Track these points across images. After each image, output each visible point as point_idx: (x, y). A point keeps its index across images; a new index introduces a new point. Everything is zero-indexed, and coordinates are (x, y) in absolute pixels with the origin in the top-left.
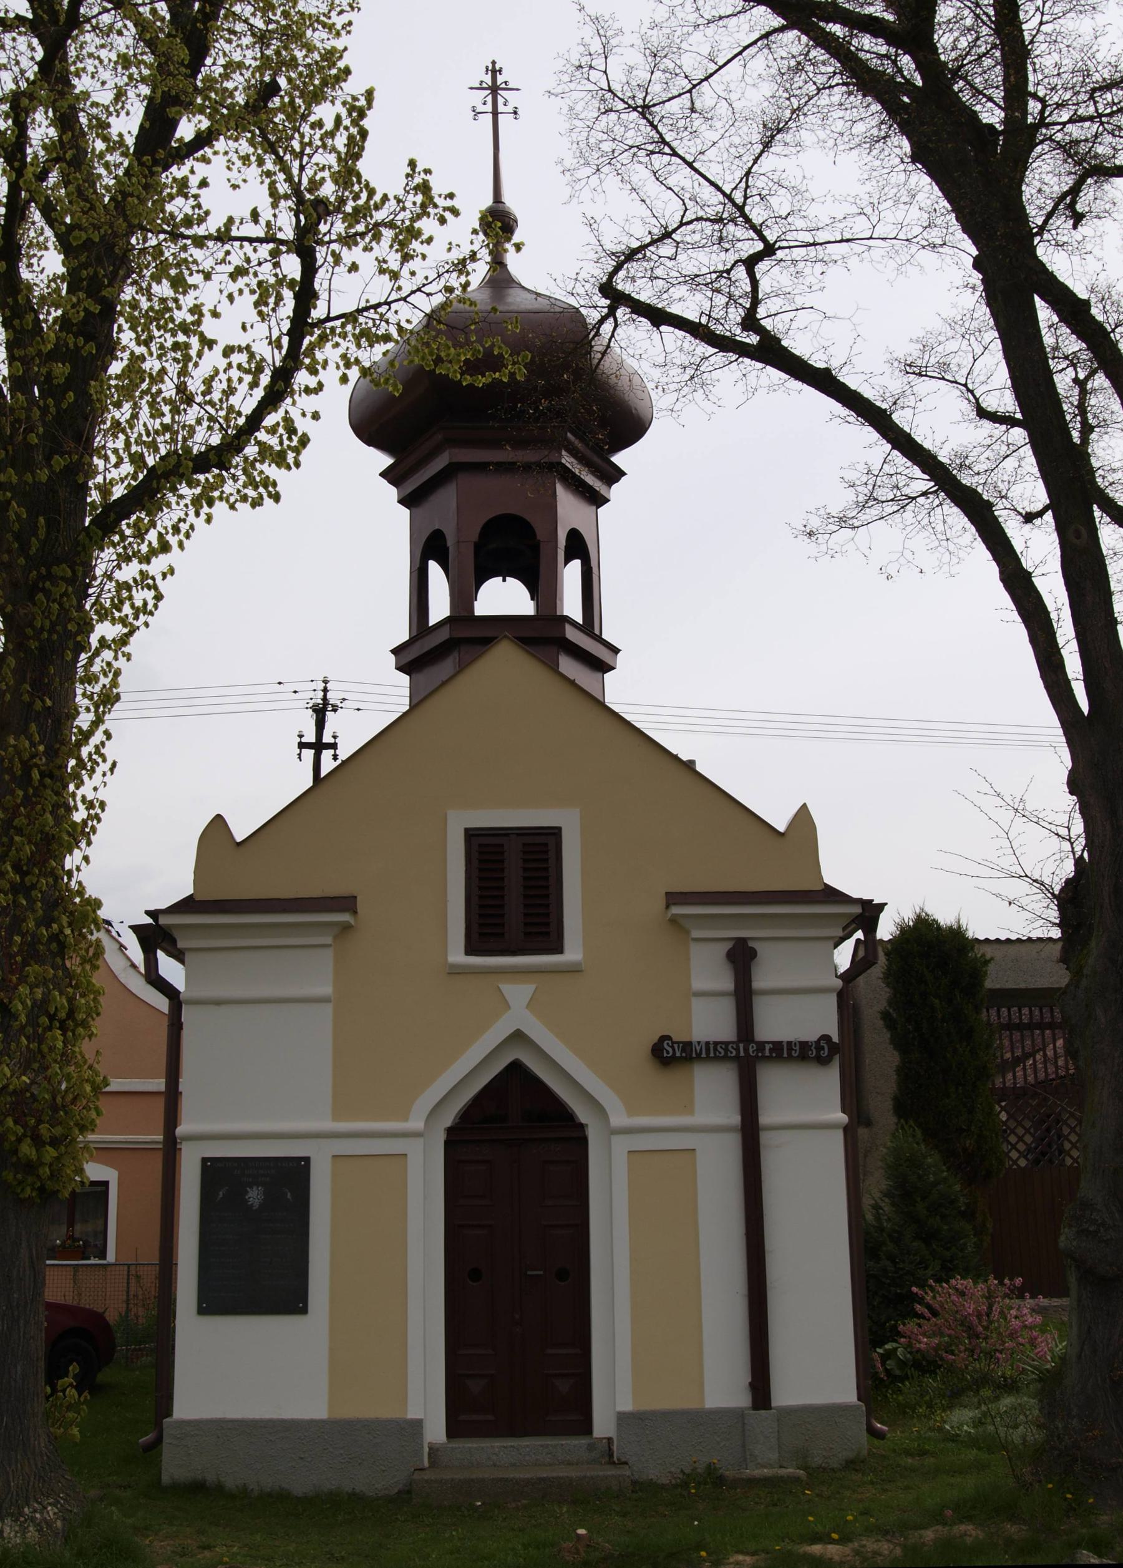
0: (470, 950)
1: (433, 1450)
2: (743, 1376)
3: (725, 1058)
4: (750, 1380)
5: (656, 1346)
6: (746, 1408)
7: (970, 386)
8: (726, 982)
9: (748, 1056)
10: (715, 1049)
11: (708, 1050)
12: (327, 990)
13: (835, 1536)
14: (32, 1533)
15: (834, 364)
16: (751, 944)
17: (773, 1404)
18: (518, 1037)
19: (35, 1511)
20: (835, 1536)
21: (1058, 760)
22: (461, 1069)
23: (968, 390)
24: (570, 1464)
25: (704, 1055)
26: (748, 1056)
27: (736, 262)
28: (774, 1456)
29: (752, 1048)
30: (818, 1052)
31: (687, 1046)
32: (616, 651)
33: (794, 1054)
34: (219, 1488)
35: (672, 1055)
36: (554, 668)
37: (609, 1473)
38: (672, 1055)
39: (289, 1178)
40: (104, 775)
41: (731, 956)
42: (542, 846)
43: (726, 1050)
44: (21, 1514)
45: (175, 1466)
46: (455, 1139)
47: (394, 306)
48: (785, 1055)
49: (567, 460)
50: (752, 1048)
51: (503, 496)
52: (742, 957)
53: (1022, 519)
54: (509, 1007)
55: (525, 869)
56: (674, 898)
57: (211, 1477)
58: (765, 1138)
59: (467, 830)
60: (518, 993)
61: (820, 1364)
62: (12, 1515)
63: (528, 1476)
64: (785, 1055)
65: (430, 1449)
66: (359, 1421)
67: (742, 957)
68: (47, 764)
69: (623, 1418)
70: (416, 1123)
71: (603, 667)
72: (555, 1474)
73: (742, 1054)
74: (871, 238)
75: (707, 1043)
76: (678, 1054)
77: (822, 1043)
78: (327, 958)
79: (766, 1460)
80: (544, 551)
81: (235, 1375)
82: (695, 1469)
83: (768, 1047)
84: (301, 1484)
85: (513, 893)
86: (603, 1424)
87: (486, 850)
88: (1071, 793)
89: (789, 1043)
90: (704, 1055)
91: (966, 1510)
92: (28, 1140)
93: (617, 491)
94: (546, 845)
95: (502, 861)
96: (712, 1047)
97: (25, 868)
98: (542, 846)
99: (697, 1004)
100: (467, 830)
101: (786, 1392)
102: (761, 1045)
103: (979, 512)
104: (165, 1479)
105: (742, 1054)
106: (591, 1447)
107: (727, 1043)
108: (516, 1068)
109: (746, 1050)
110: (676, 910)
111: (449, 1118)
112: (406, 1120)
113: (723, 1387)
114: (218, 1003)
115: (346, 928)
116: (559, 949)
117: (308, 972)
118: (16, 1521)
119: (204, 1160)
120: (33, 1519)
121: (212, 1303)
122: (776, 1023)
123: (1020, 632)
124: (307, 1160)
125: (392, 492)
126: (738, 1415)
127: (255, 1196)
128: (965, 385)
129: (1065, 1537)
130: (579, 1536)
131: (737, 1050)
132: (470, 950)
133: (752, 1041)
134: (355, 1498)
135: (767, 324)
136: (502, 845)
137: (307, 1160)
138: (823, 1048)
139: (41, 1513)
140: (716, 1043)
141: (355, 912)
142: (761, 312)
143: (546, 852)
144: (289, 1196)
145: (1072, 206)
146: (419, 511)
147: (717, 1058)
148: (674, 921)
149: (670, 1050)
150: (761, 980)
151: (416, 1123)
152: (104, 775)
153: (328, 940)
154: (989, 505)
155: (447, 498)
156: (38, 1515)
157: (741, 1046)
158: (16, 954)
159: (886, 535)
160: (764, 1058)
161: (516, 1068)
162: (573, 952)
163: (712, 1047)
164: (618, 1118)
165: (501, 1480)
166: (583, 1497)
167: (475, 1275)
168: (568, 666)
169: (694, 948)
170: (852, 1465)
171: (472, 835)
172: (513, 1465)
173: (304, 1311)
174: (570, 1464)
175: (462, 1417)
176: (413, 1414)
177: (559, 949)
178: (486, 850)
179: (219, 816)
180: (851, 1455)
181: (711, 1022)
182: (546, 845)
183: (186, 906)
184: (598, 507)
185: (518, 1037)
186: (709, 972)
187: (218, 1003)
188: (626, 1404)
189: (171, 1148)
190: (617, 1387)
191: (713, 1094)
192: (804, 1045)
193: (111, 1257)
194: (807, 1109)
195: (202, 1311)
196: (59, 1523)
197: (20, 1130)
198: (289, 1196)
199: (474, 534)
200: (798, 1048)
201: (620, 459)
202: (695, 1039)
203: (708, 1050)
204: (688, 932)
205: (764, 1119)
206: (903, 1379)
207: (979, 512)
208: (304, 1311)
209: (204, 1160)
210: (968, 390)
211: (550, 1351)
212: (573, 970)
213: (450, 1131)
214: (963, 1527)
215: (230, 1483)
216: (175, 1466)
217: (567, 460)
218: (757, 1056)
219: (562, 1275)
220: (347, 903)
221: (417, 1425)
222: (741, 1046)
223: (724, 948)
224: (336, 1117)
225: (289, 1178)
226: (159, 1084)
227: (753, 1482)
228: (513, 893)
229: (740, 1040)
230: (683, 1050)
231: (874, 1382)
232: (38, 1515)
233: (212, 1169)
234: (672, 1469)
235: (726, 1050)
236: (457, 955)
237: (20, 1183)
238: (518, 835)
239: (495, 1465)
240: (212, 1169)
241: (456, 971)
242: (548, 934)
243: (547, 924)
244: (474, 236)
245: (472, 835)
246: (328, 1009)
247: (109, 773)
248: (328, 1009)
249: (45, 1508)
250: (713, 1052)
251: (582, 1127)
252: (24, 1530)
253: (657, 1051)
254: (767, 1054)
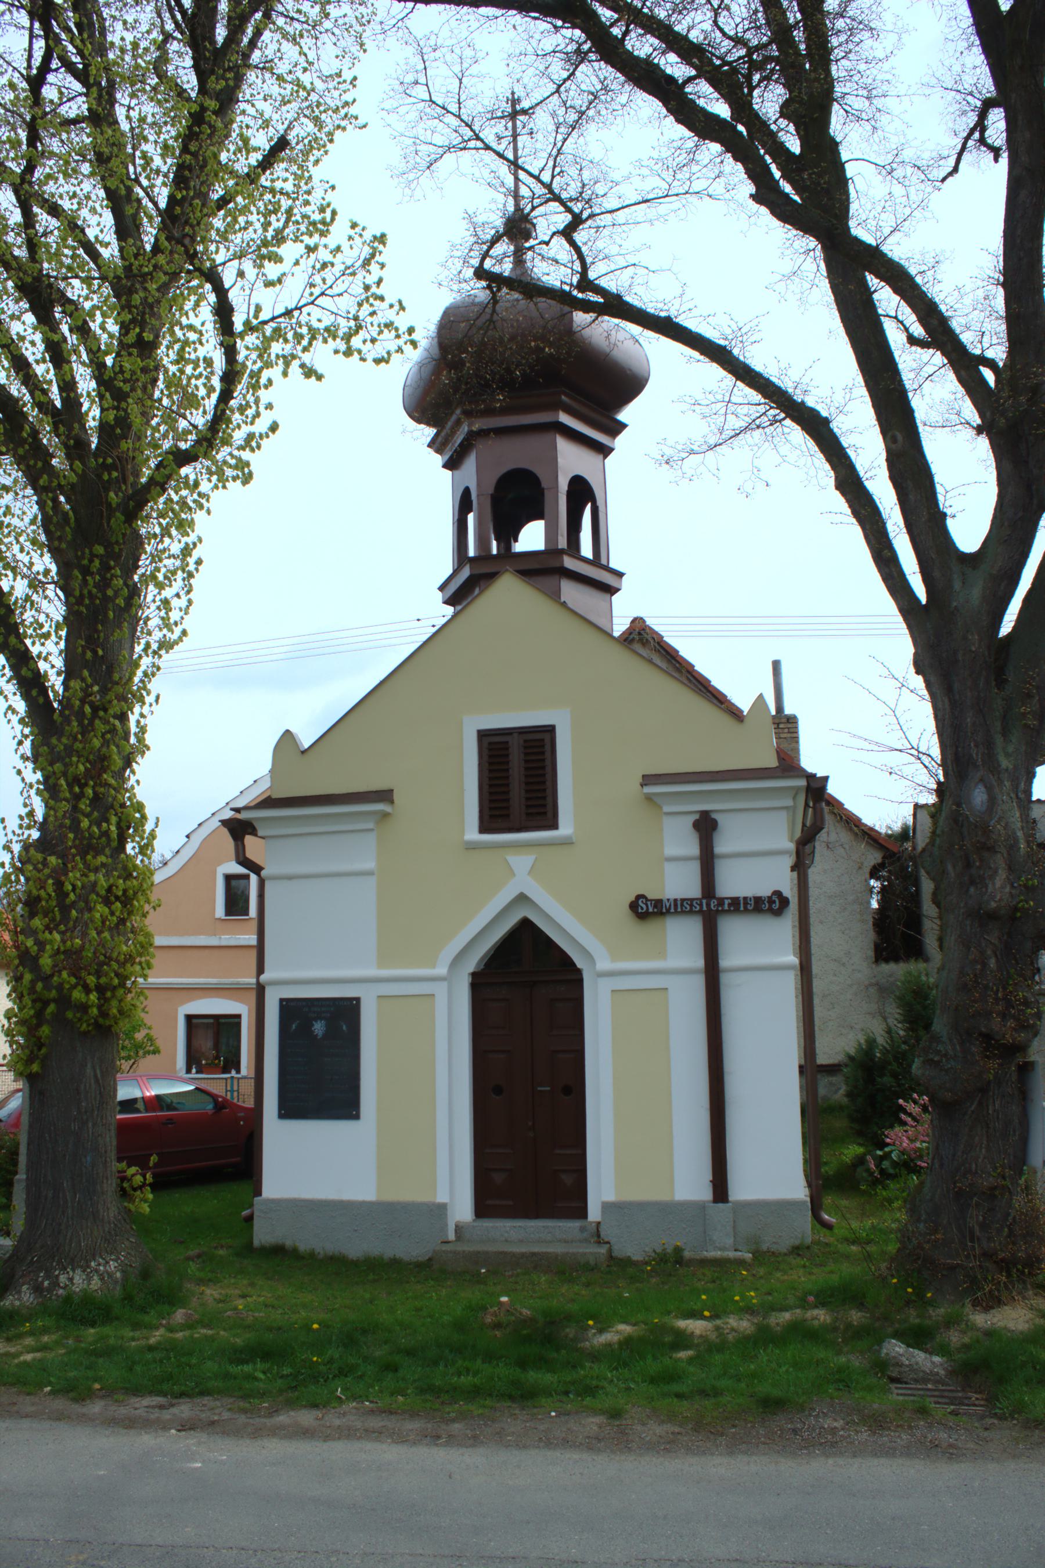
0: (484, 829)
1: (459, 1228)
2: (706, 1174)
3: (691, 912)
4: (711, 1178)
5: (637, 1149)
6: (708, 1202)
7: (900, 318)
8: (692, 847)
9: (711, 910)
10: (682, 905)
11: (676, 905)
12: (370, 865)
13: (706, 1313)
14: (96, 1283)
15: (673, 313)
16: (714, 816)
17: (730, 1199)
18: (522, 899)
19: (99, 1265)
20: (706, 1313)
21: (901, 647)
22: (475, 927)
23: (898, 321)
24: (566, 1242)
25: (672, 910)
26: (711, 910)
27: (554, 234)
28: (730, 1241)
29: (713, 903)
30: (770, 906)
31: (658, 903)
32: (620, 575)
33: (750, 908)
34: (295, 1250)
35: (647, 910)
36: (555, 595)
37: (587, 1251)
38: (647, 910)
39: (344, 1014)
40: (151, 705)
41: (696, 825)
42: (538, 744)
43: (691, 905)
44: (89, 1266)
45: (263, 1234)
46: (479, 983)
47: (305, 310)
48: (742, 908)
49: (564, 418)
50: (713, 903)
51: (515, 454)
52: (706, 827)
53: (975, 432)
54: (514, 875)
55: (526, 761)
56: (648, 780)
57: (288, 1243)
58: (725, 979)
59: (479, 732)
60: (521, 862)
61: (773, 1166)
62: (81, 1267)
63: (523, 1250)
64: (742, 908)
65: (456, 1226)
66: (399, 1203)
67: (706, 827)
68: (100, 700)
69: (607, 1207)
70: (442, 970)
71: (611, 590)
72: (544, 1250)
73: (705, 908)
74: (667, 196)
75: (676, 900)
76: (651, 910)
77: (774, 898)
78: (371, 839)
79: (722, 1244)
80: (548, 495)
81: (305, 1165)
82: (664, 1250)
83: (727, 902)
84: (355, 1249)
85: (518, 781)
86: (594, 1213)
87: (494, 747)
88: (917, 673)
89: (745, 898)
90: (672, 910)
91: (825, 1298)
92: (80, 988)
93: (620, 442)
94: (543, 740)
95: (507, 755)
96: (679, 903)
97: (83, 781)
98: (538, 744)
99: (668, 867)
100: (479, 732)
101: (745, 1187)
102: (721, 901)
103: (817, 428)
104: (256, 1243)
105: (705, 908)
106: (582, 1229)
107: (692, 900)
108: (526, 924)
109: (708, 905)
110: (647, 790)
111: (472, 964)
112: (434, 967)
113: (690, 1184)
114: (290, 878)
115: (385, 815)
116: (554, 825)
117: (356, 851)
118: (84, 1271)
119: (281, 1000)
120: (97, 1271)
121: (289, 1110)
122: (733, 882)
123: (855, 533)
124: (358, 1000)
125: (438, 460)
126: (700, 1207)
127: (319, 1028)
128: (896, 317)
129: (897, 1325)
130: (501, 1303)
131: (701, 905)
132: (484, 829)
133: (714, 897)
134: (395, 1263)
135: (603, 283)
136: (507, 742)
137: (358, 1000)
138: (774, 902)
139: (105, 1266)
140: (683, 900)
141: (392, 802)
142: (592, 275)
143: (543, 746)
144: (344, 1028)
145: (982, 141)
146: (456, 472)
147: (683, 912)
148: (649, 798)
149: (644, 906)
150: (722, 845)
151: (442, 970)
152: (151, 705)
153: (371, 825)
154: (826, 421)
155: (470, 464)
156: (102, 1268)
157: (704, 901)
158: (71, 848)
159: (736, 457)
160: (724, 911)
161: (526, 924)
162: (566, 828)
163: (679, 903)
164: (604, 964)
165: (501, 1253)
166: (564, 1269)
167: (498, 1090)
168: (570, 591)
169: (667, 821)
170: (797, 1250)
171: (483, 735)
172: (521, 1241)
173: (357, 1117)
174: (566, 1242)
175: (489, 1202)
176: (442, 1198)
177: (554, 825)
178: (494, 747)
179: (287, 731)
180: (797, 1242)
181: (681, 882)
182: (543, 740)
183: (268, 802)
184: (605, 457)
185: (522, 899)
186: (680, 841)
187: (290, 878)
188: (610, 1196)
189: (260, 990)
190: (604, 1184)
191: (682, 940)
192: (758, 900)
193: (244, 1071)
194: (759, 951)
195: (282, 1116)
196: (118, 1275)
197: (73, 980)
198: (344, 1028)
199: (491, 490)
200: (752, 902)
201: (622, 416)
202: (664, 898)
203: (676, 905)
204: (661, 808)
205: (724, 962)
206: (893, 1177)
207: (817, 428)
208: (357, 1117)
209: (281, 1000)
210: (898, 321)
211: (558, 1151)
212: (566, 842)
213: (474, 975)
214: (815, 1312)
215: (303, 1247)
216: (263, 1234)
217: (564, 418)
218: (717, 910)
219: (567, 1090)
220: (385, 796)
221: (441, 1210)
222: (704, 901)
223: (691, 819)
224: (381, 963)
225: (344, 1014)
226: (252, 939)
227: (704, 1262)
228: (518, 781)
229: (703, 897)
230: (655, 906)
231: (823, 1181)
232: (102, 1268)
233: (287, 1007)
234: (647, 1249)
235: (691, 905)
236: (472, 833)
237: (80, 1019)
238: (520, 733)
239: (506, 1241)
240: (287, 1007)
241: (472, 847)
242: (545, 813)
243: (545, 806)
244: (351, 242)
245: (483, 735)
246: (372, 882)
247: (154, 704)
248: (372, 882)
249: (107, 1263)
250: (681, 907)
251: (579, 972)
252: (89, 1279)
253: (634, 906)
254: (726, 907)
